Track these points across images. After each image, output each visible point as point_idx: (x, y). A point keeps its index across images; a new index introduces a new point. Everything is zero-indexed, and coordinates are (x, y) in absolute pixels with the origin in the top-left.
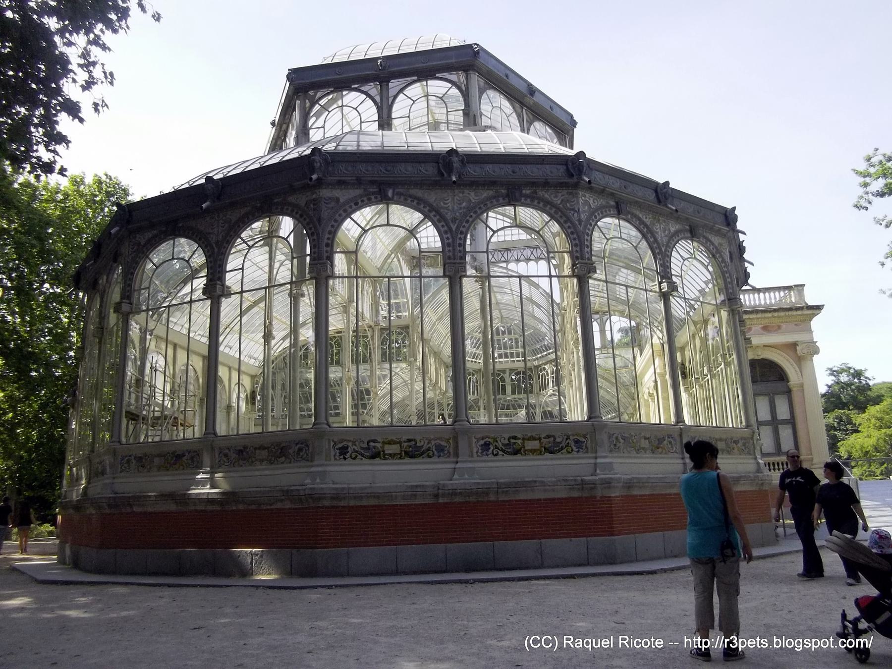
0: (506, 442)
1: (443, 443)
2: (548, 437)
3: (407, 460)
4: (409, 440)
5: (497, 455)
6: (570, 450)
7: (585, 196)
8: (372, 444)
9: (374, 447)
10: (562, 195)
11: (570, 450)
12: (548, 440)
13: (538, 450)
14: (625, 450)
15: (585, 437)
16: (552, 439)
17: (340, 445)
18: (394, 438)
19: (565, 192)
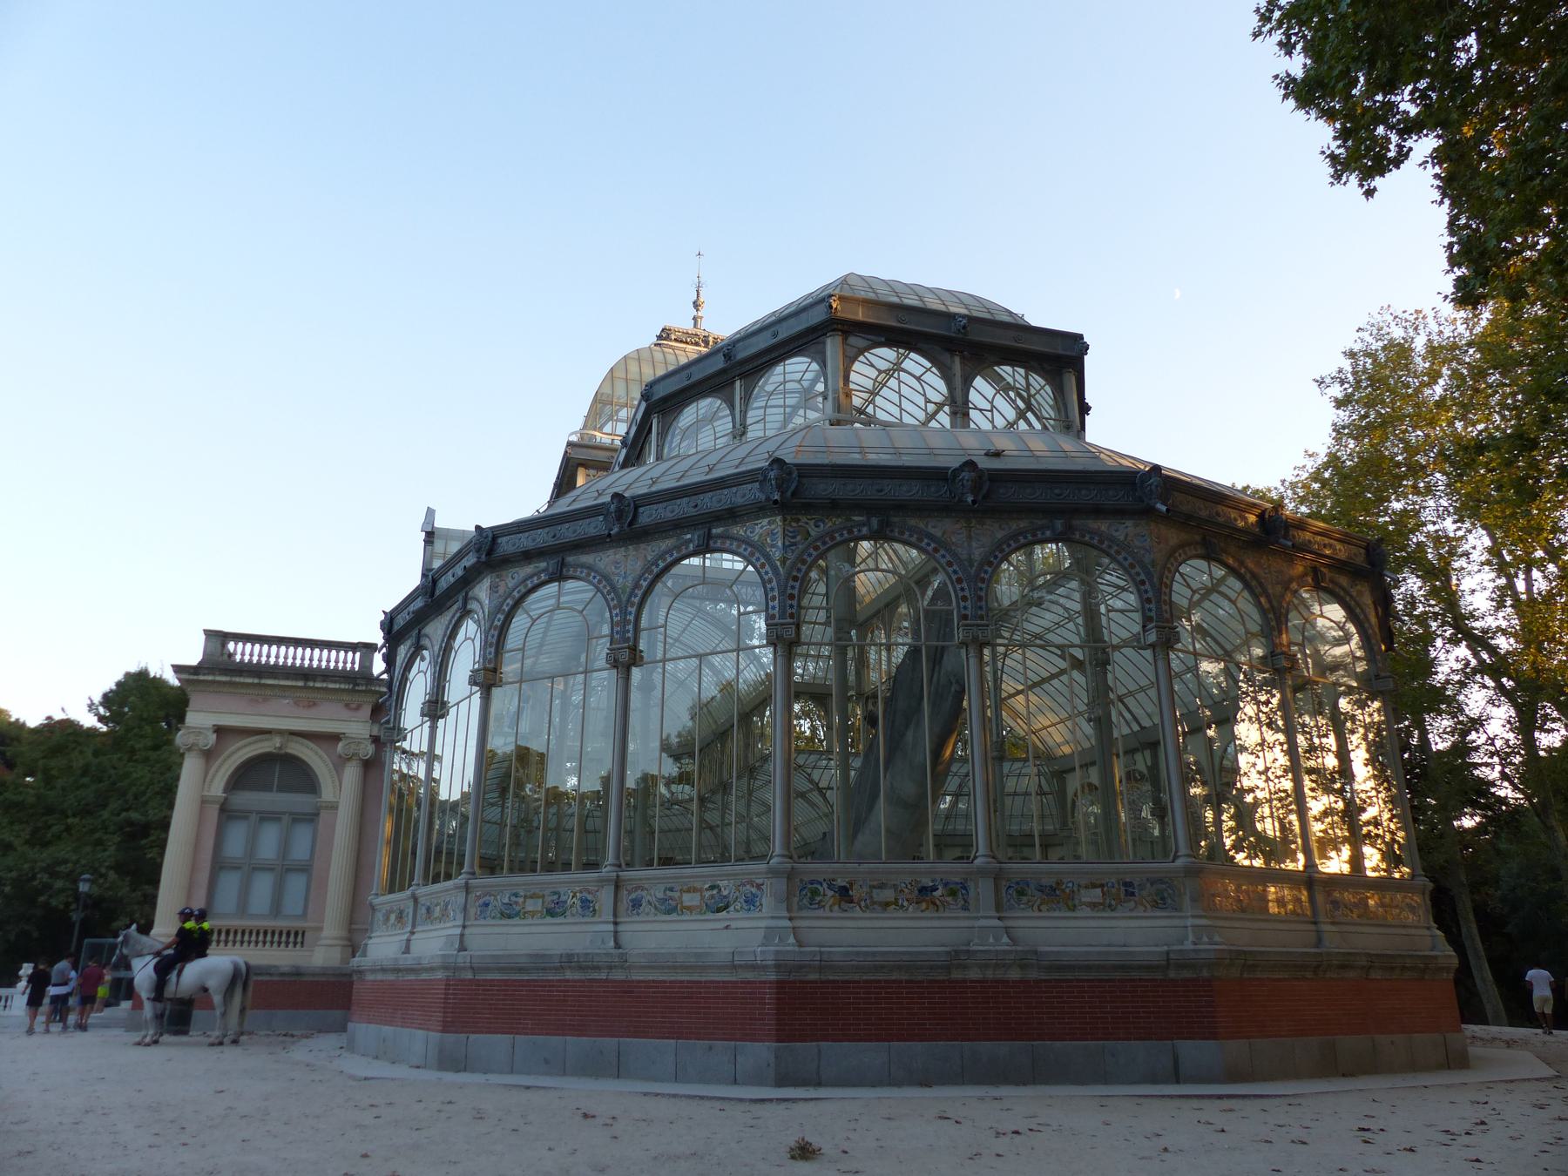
0: (660, 895)
1: (590, 897)
2: (712, 888)
3: (549, 920)
4: (555, 893)
5: (648, 914)
6: (738, 908)
7: (799, 520)
8: (513, 898)
9: (516, 903)
10: (761, 528)
11: (738, 908)
12: (710, 893)
13: (697, 907)
14: (836, 907)
15: (759, 887)
16: (715, 892)
17: (481, 901)
18: (537, 891)
19: (765, 521)
